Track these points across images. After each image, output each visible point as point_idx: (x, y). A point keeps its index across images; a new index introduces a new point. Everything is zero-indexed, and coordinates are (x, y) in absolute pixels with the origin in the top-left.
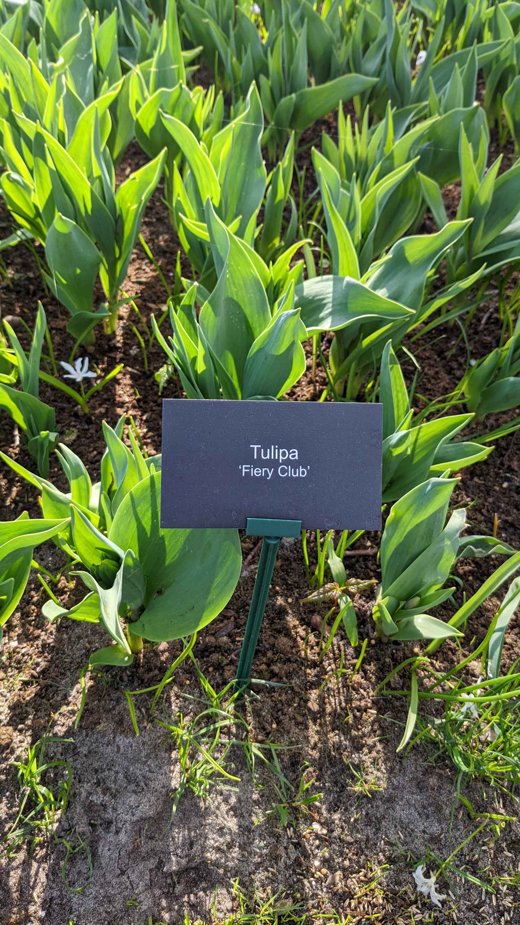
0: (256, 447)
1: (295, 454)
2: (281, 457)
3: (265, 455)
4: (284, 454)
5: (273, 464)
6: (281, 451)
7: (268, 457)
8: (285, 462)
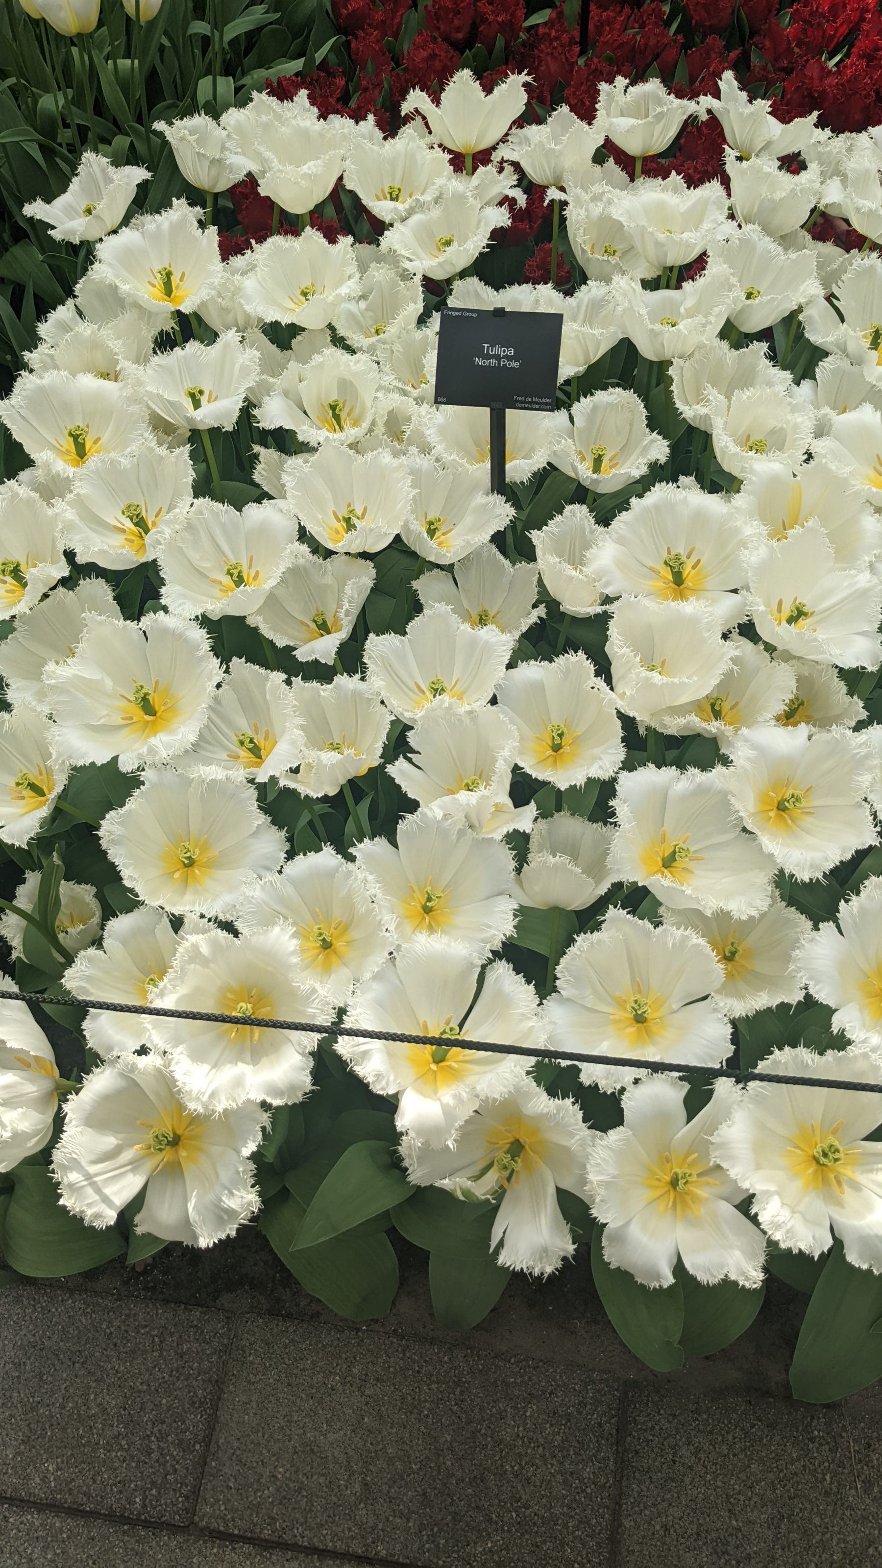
4: (504, 351)
8: (504, 357)
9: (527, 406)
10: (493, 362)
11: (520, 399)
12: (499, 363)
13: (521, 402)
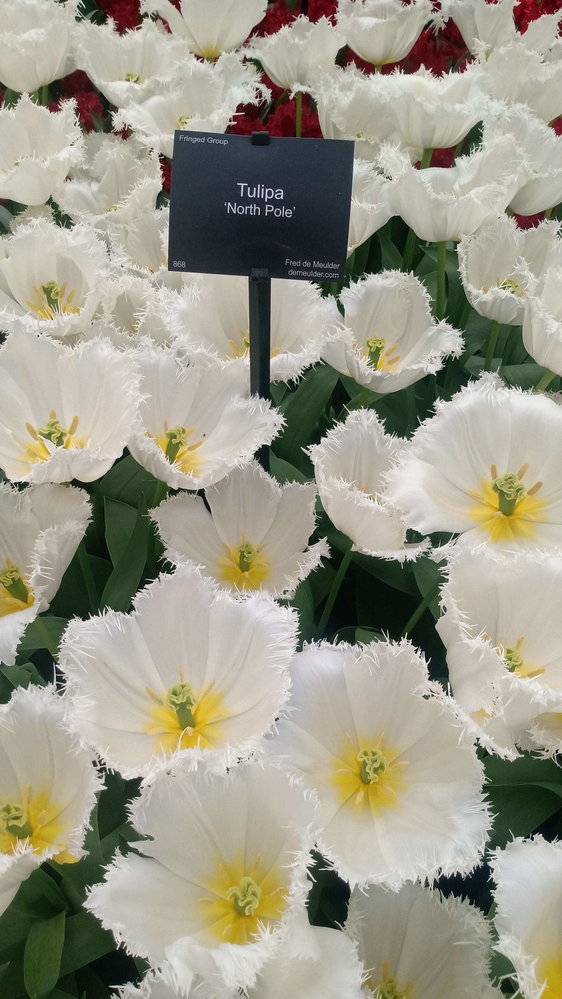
0: (242, 185)
3: (252, 193)
4: (270, 194)
5: (260, 202)
6: (267, 190)
7: (254, 195)
8: (271, 202)
9: (304, 273)
11: (294, 263)
12: (263, 211)
13: (296, 268)
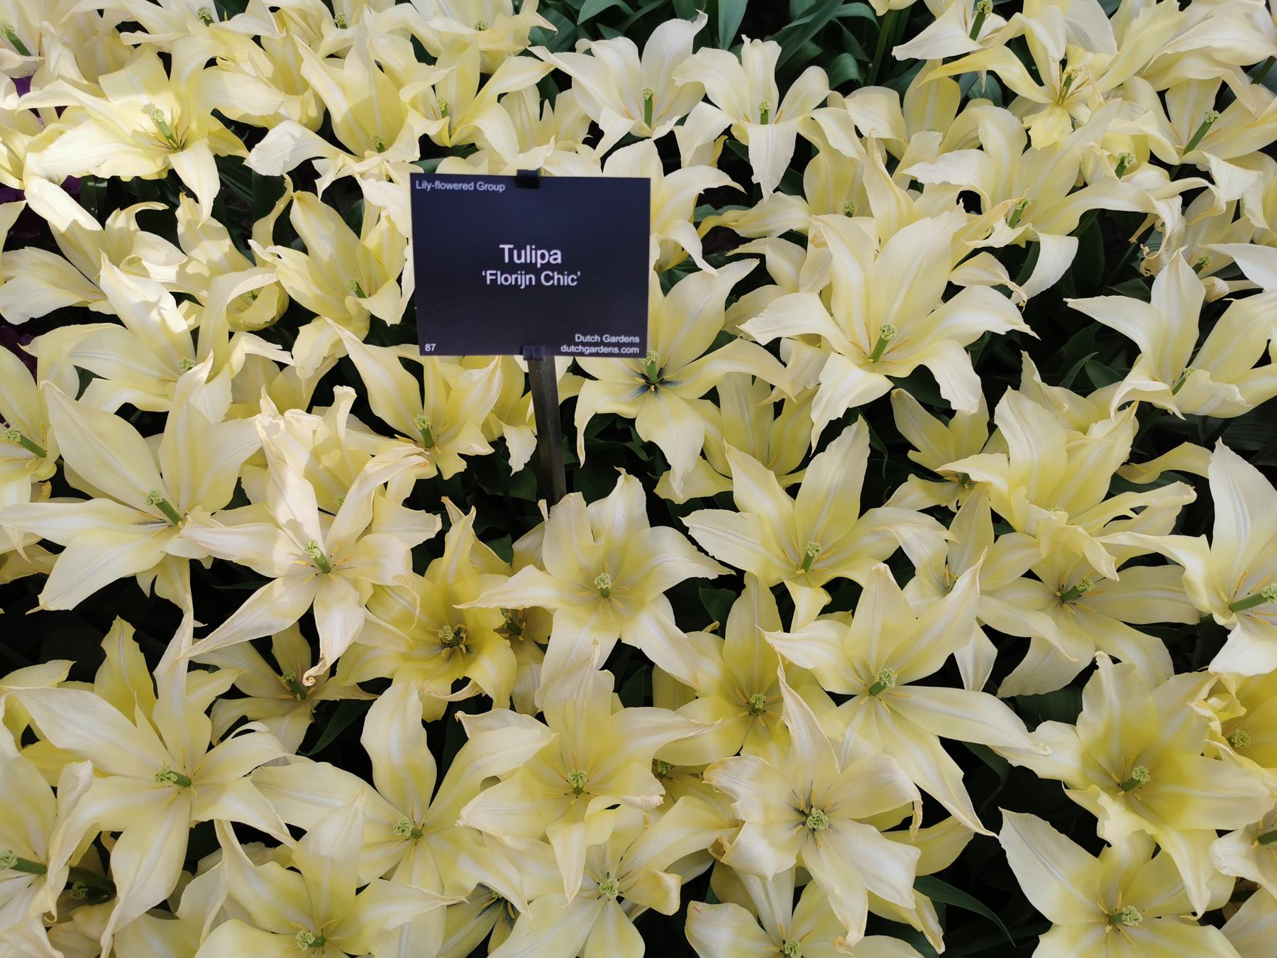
0: (506, 247)
1: (557, 257)
2: (540, 261)
3: (519, 258)
4: (543, 257)
5: (530, 268)
8: (544, 267)
10: (524, 280)
12: (538, 279)
